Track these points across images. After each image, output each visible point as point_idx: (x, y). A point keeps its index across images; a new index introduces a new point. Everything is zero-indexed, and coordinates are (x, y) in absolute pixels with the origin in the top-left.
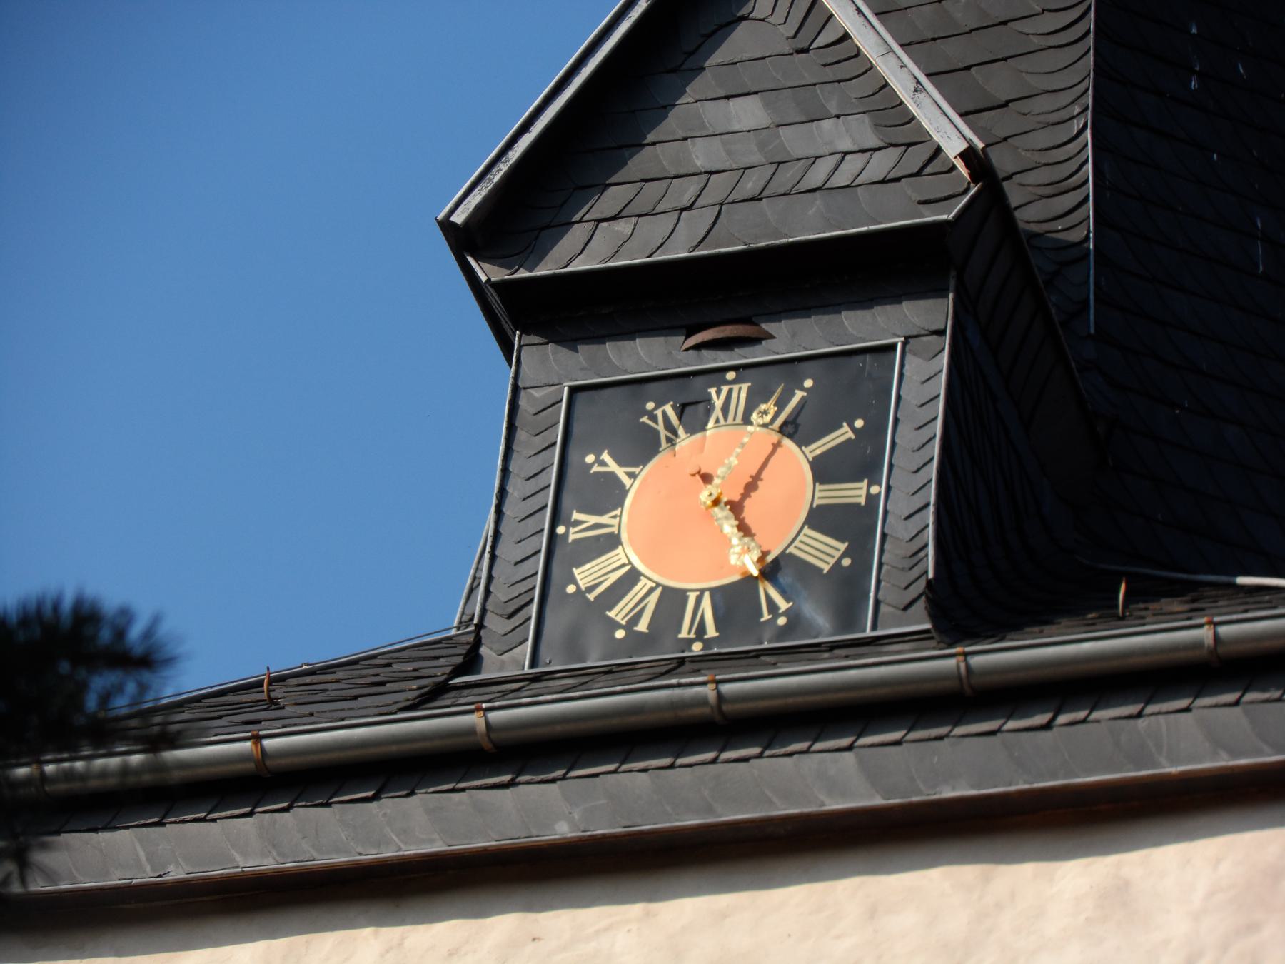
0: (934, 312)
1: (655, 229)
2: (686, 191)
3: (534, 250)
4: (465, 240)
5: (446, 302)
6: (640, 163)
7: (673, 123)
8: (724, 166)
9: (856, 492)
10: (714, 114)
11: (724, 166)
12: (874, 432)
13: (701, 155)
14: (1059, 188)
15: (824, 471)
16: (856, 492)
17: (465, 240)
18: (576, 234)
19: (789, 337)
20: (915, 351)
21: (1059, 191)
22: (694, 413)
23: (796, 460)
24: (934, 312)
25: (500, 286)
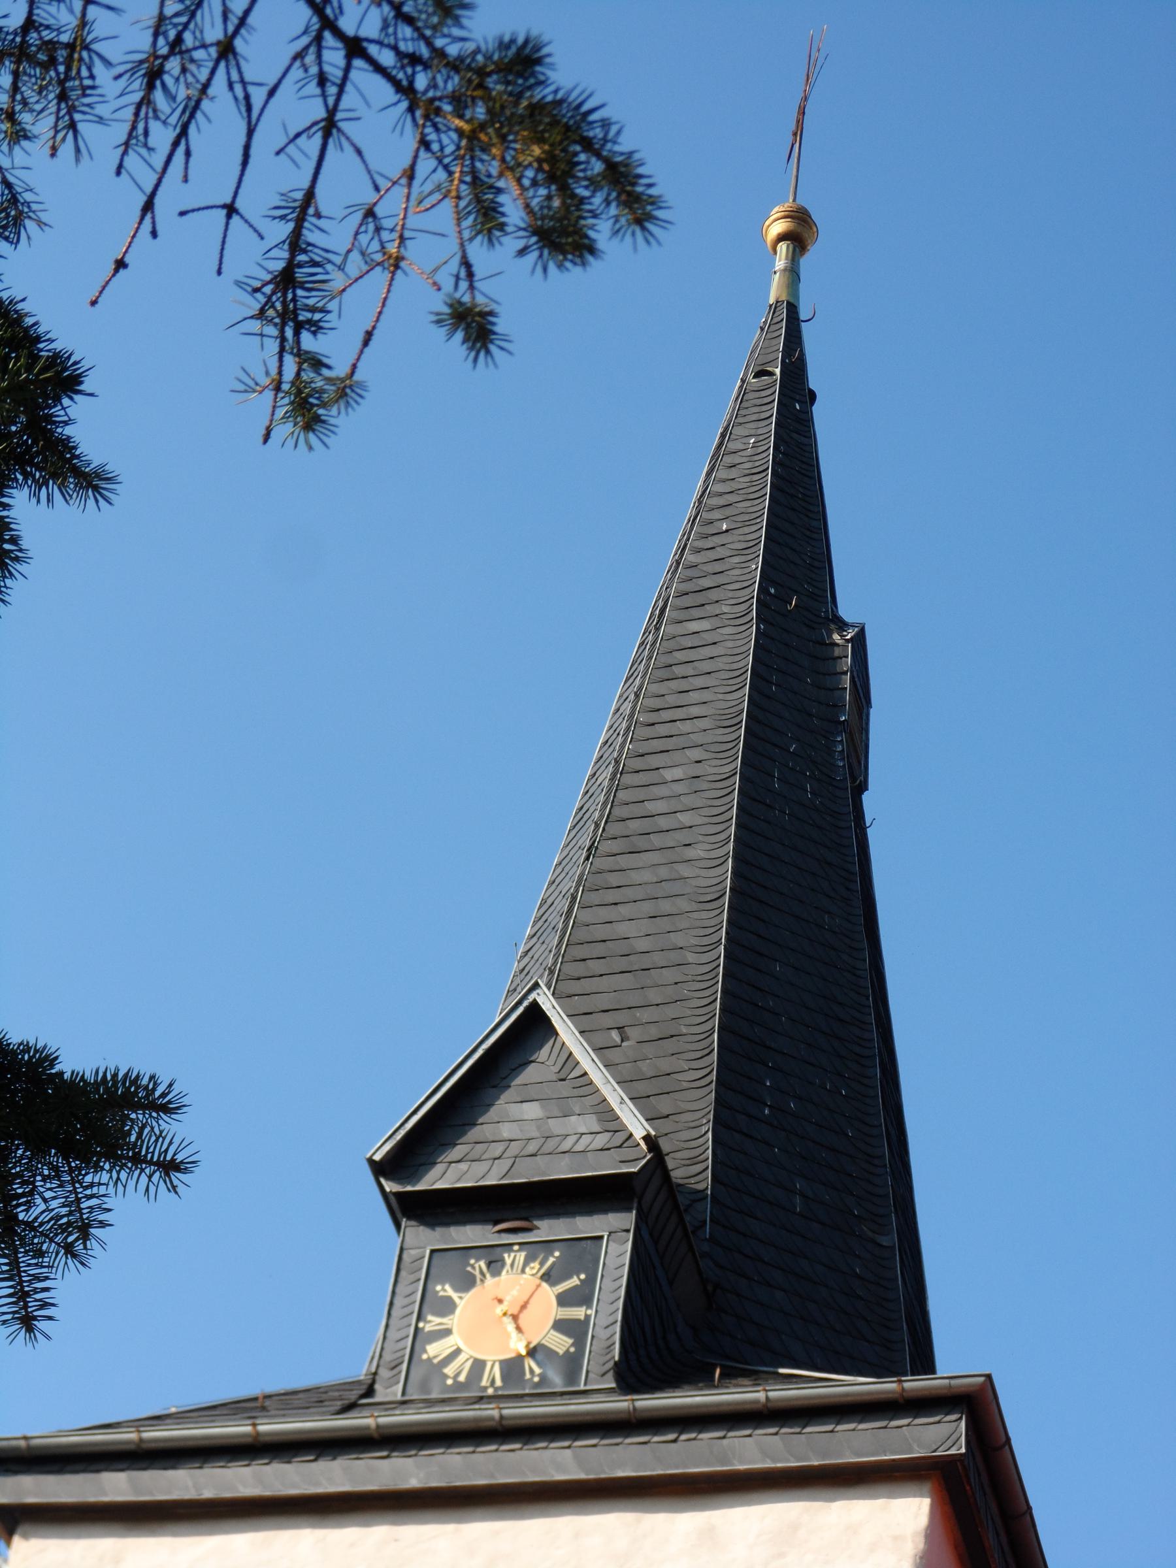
0: (627, 1219)
1: (481, 1168)
2: (498, 1149)
3: (415, 1177)
4: (380, 1169)
5: (368, 1200)
6: (474, 1133)
7: (493, 1113)
8: (513, 1140)
9: (579, 1313)
10: (516, 1110)
11: (513, 1140)
12: (590, 1282)
13: (506, 1131)
14: (693, 1161)
15: (563, 1300)
16: (579, 1313)
17: (380, 1169)
18: (438, 1169)
19: (548, 1229)
20: (614, 1237)
21: (694, 1162)
22: (496, 1266)
23: (549, 1293)
24: (627, 1219)
25: (398, 1195)
